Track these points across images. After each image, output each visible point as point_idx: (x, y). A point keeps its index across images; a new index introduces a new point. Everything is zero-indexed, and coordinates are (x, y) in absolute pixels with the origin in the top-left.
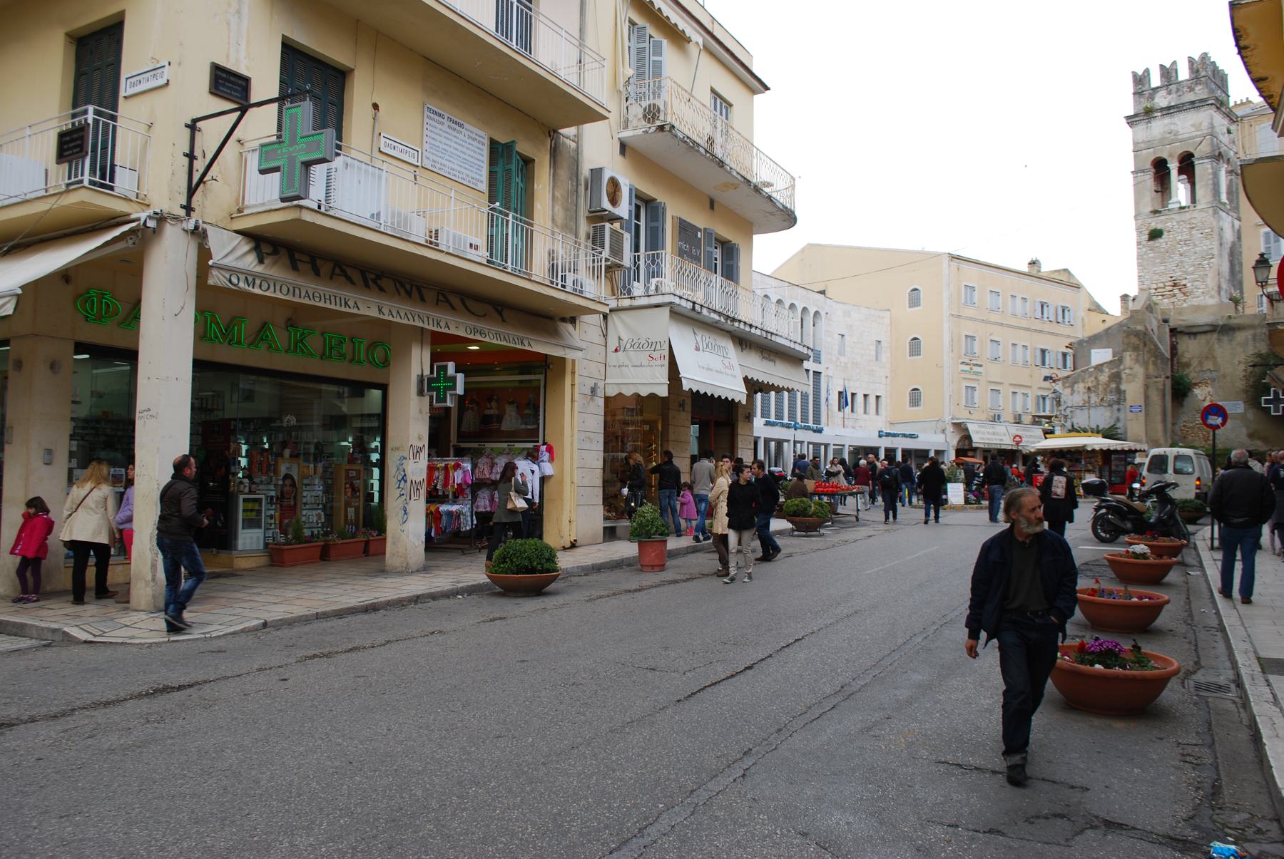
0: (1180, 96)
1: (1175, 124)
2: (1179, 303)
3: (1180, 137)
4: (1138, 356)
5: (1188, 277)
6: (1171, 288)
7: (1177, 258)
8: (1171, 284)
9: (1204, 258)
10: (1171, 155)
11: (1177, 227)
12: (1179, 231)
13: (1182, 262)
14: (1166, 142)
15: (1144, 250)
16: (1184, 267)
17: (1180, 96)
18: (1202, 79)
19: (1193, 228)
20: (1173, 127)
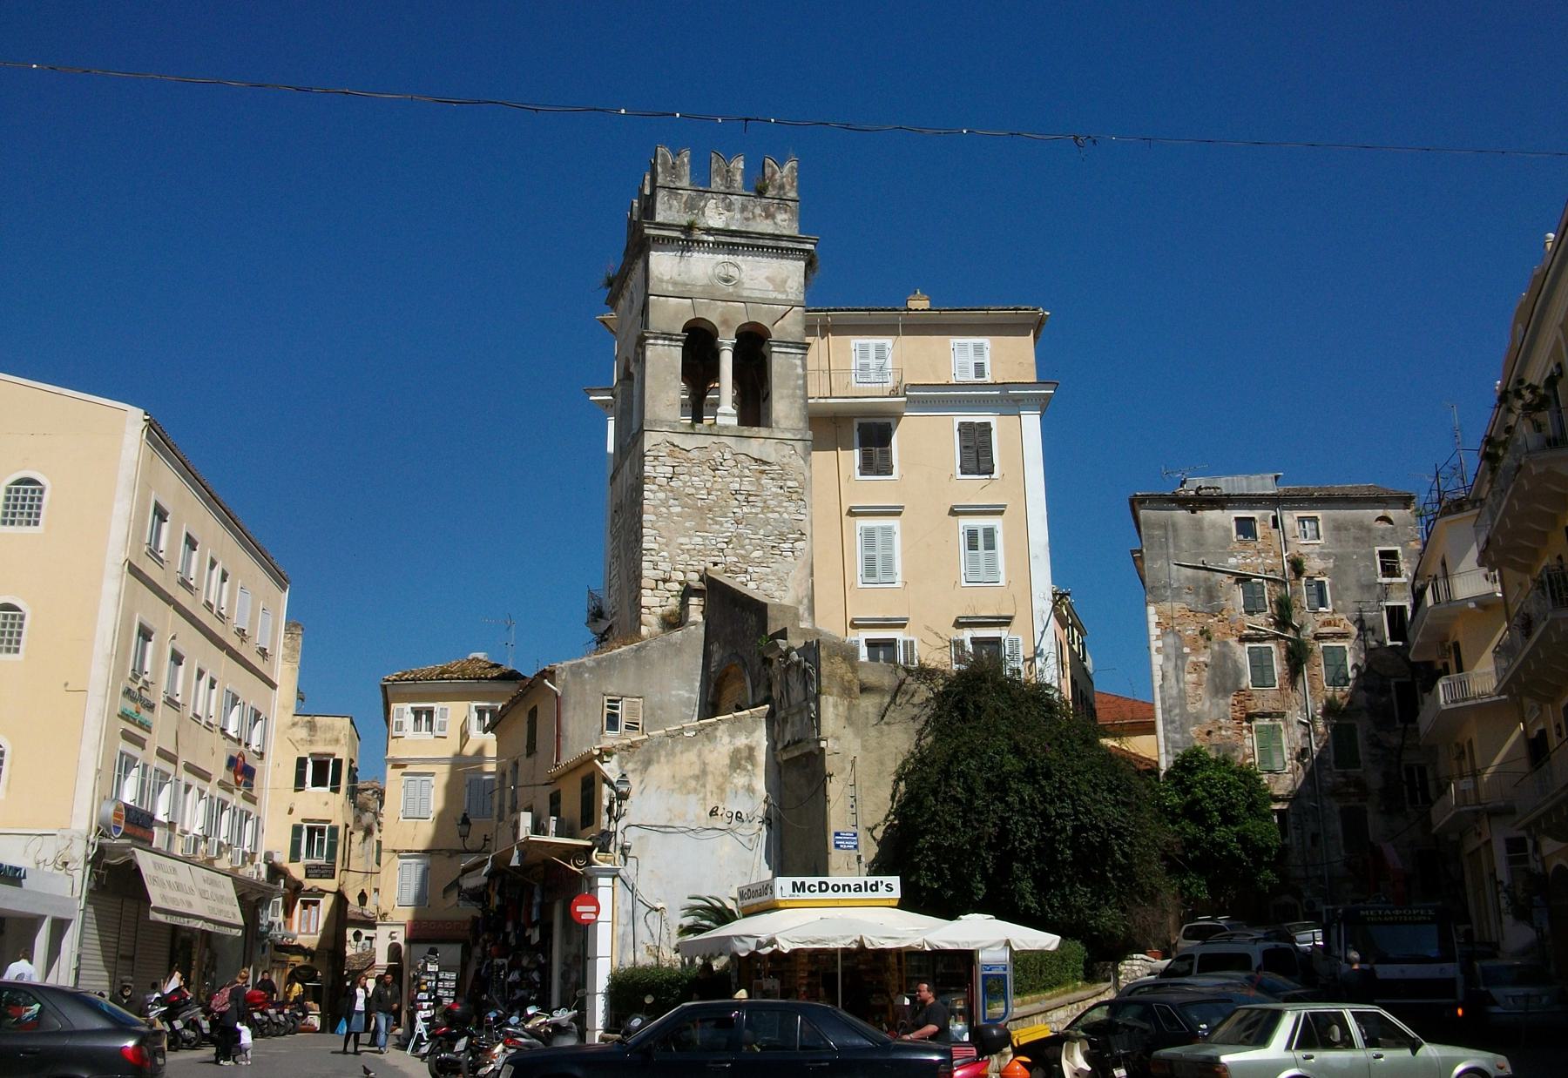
0: (747, 219)
1: (737, 266)
3: (746, 293)
4: (850, 708)
5: (750, 570)
7: (729, 527)
9: (783, 537)
10: (725, 322)
11: (732, 463)
12: (736, 471)
13: (739, 536)
14: (718, 295)
15: (662, 495)
16: (743, 547)
17: (747, 219)
18: (790, 203)
19: (763, 472)
20: (733, 271)
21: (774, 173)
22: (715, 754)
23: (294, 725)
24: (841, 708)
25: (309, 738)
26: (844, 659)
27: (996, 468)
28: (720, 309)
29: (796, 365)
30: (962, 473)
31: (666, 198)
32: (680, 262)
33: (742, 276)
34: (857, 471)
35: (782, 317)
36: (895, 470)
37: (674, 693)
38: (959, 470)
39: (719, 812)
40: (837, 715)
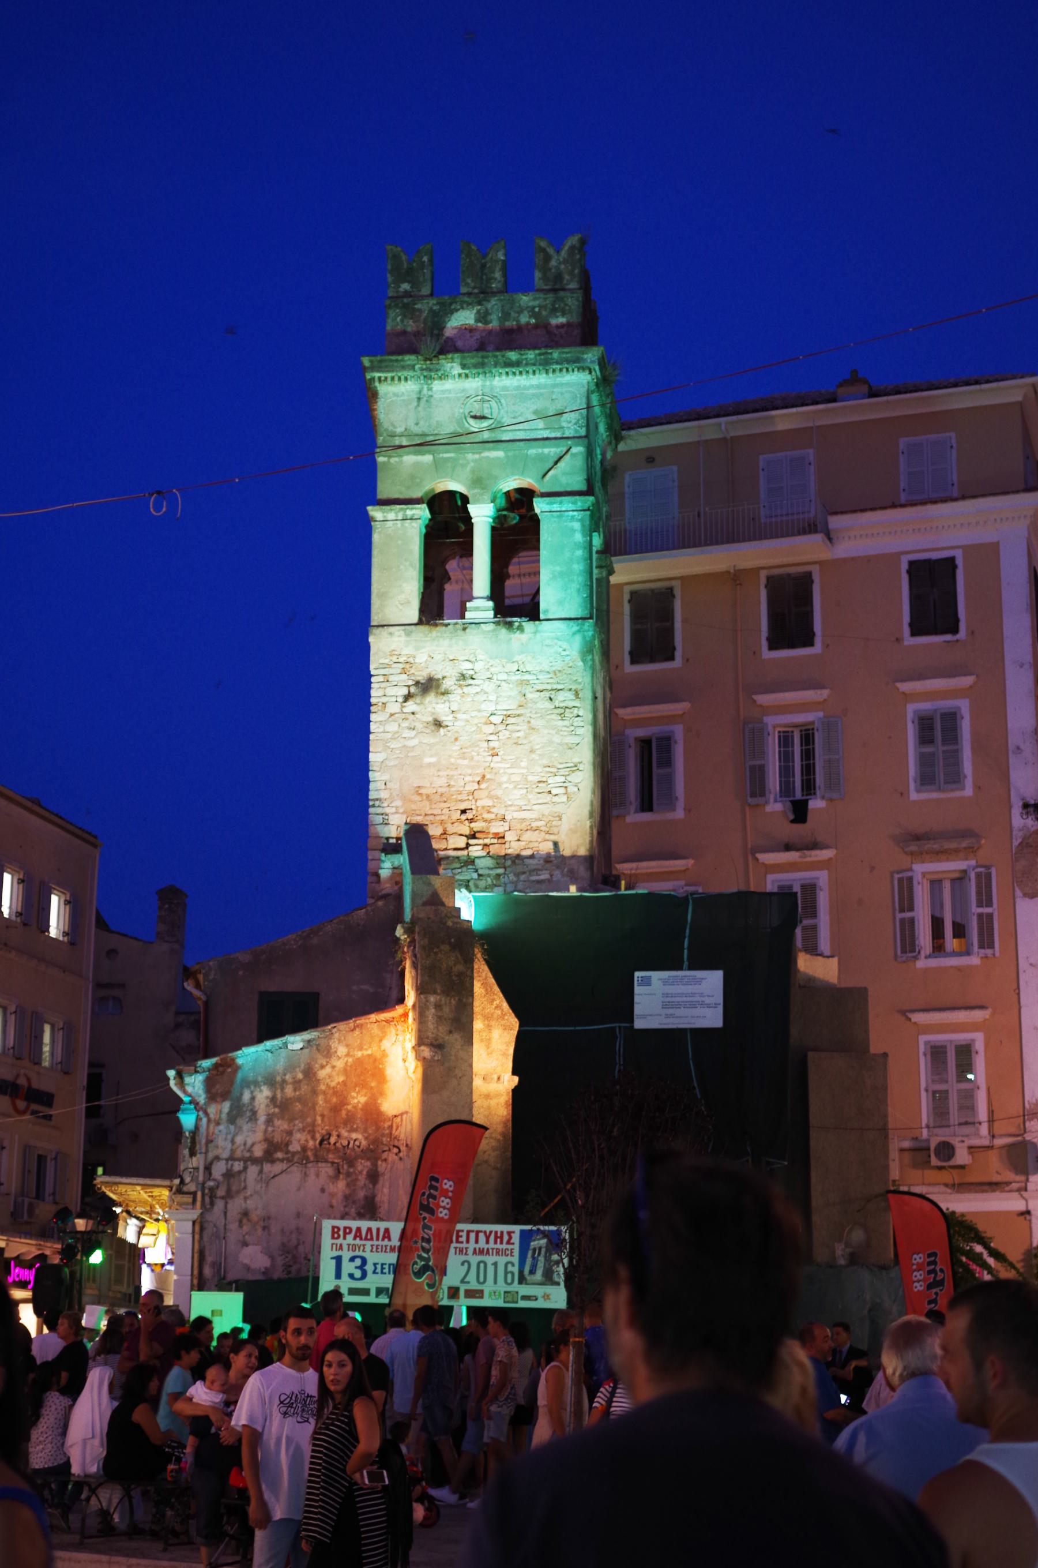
6: (462, 842)
21: (548, 258)
22: (328, 1070)
23: (178, 1026)
24: (446, 1010)
26: (454, 947)
28: (472, 464)
29: (573, 530)
31: (399, 319)
32: (418, 405)
33: (502, 412)
34: (765, 644)
35: (556, 463)
37: (355, 988)
38: (907, 630)
39: (333, 1140)
40: (440, 1017)
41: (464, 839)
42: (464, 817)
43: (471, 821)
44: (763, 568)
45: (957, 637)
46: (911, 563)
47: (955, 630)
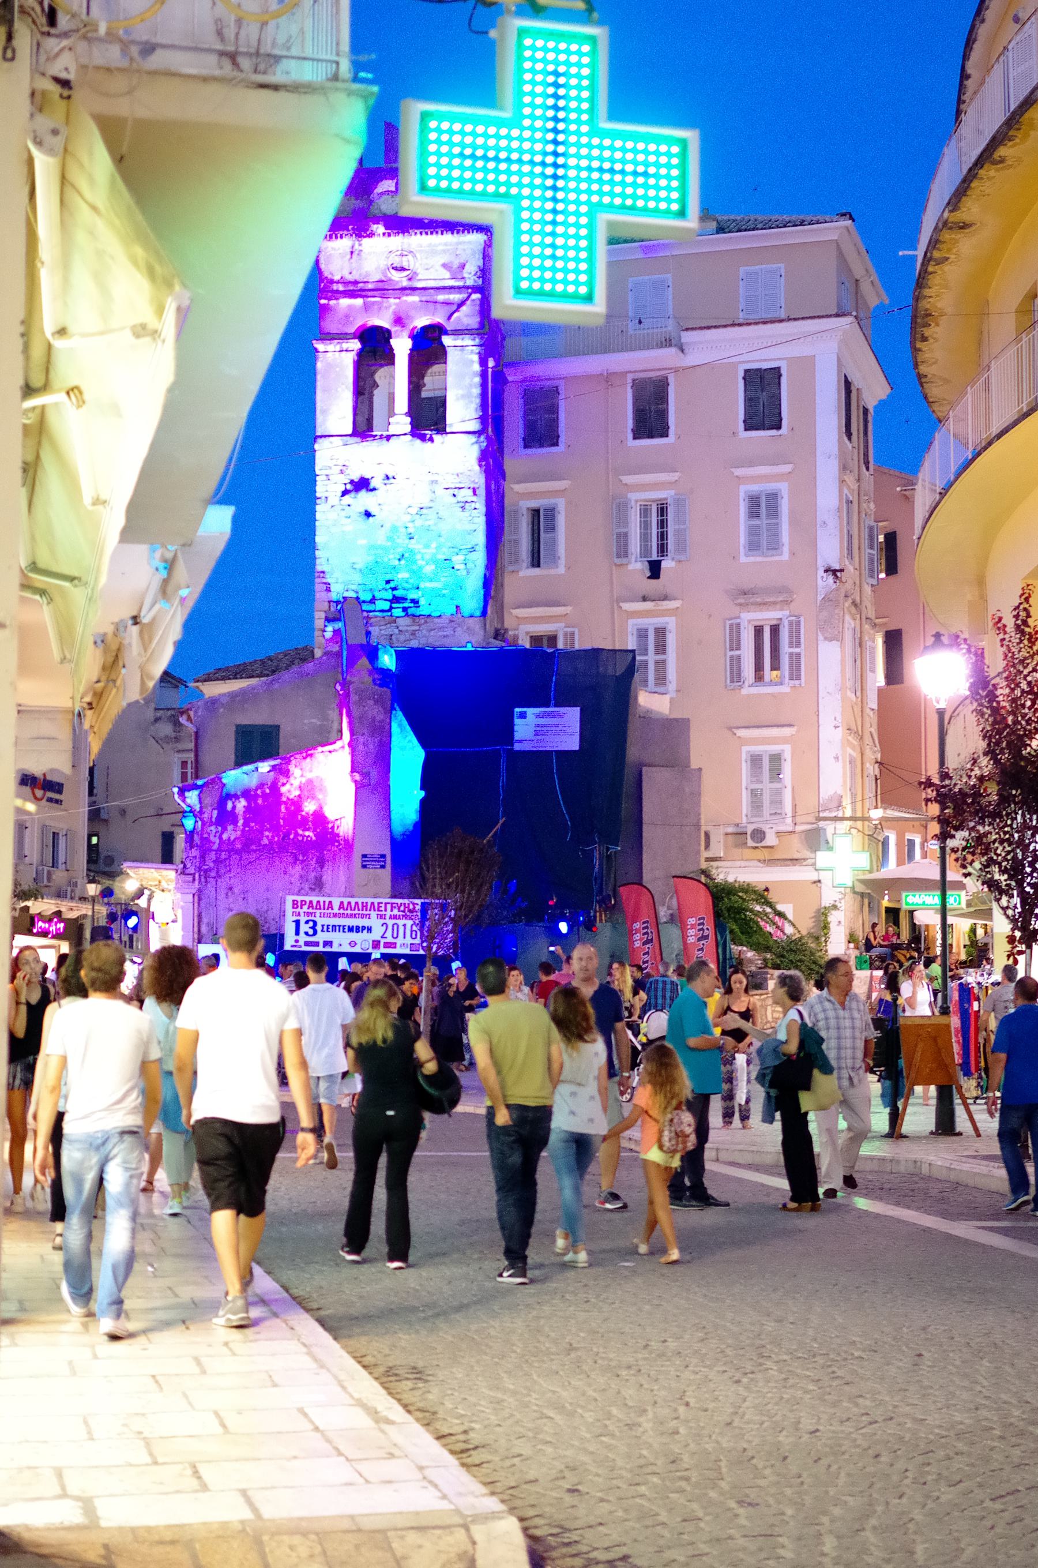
2: (402, 638)
5: (422, 586)
6: (386, 605)
8: (389, 595)
22: (288, 786)
23: (157, 720)
24: (371, 746)
25: (173, 735)
27: (784, 423)
29: (473, 362)
30: (746, 430)
33: (417, 265)
34: (630, 435)
36: (672, 431)
38: (741, 426)
41: (388, 603)
42: (388, 586)
43: (394, 589)
44: (631, 372)
45: (780, 432)
46: (746, 371)
47: (779, 427)
